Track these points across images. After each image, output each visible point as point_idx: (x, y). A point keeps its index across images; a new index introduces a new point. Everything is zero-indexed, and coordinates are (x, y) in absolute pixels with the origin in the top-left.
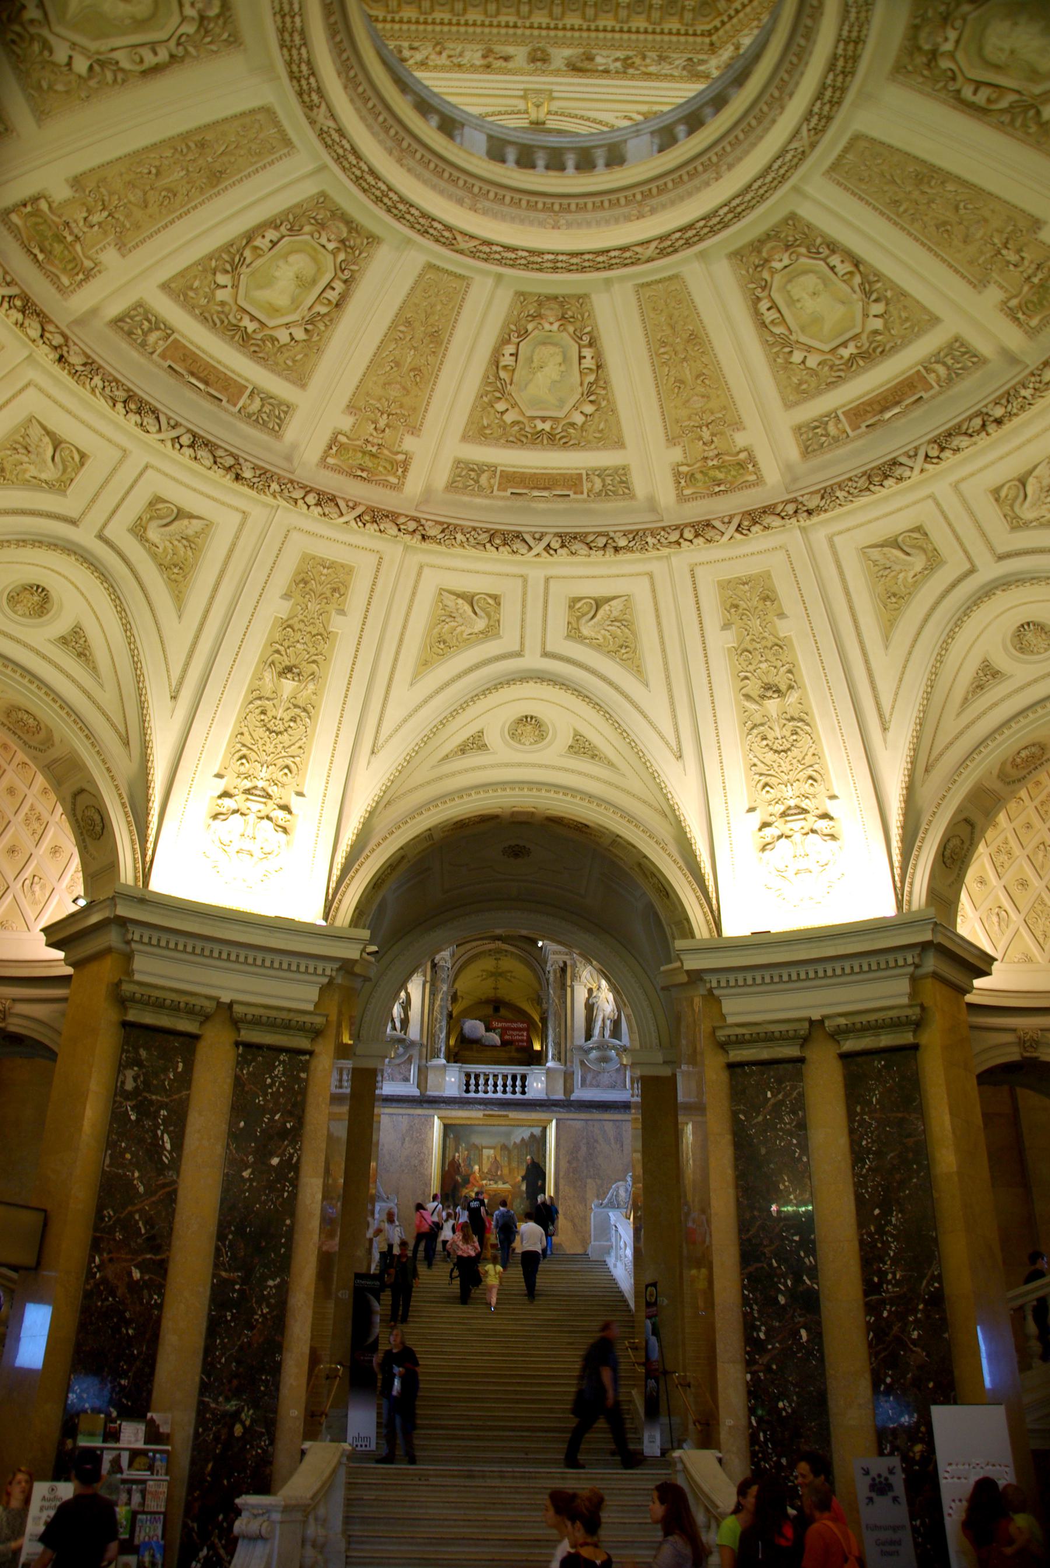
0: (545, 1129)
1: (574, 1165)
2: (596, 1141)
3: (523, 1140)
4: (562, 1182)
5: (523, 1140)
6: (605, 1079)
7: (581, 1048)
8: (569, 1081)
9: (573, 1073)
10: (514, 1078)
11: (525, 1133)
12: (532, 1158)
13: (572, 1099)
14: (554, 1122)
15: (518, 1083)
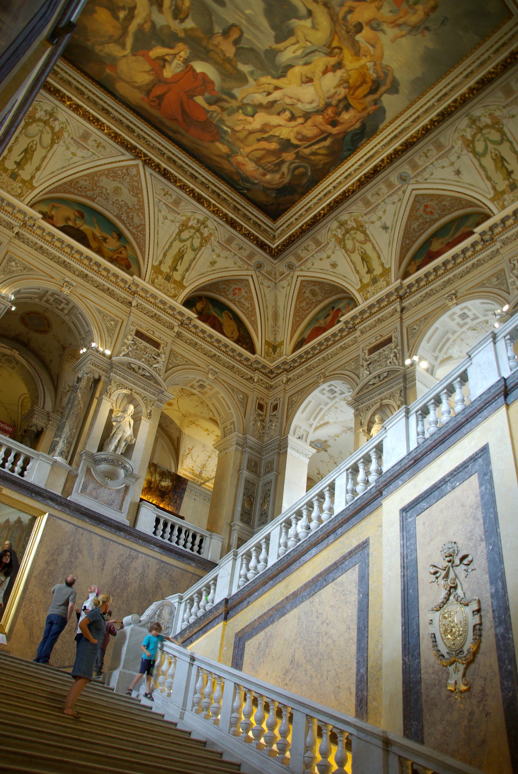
0: (34, 519)
1: (52, 568)
2: (80, 551)
3: (8, 521)
4: (33, 581)
5: (8, 521)
6: (104, 494)
7: (91, 456)
8: (70, 482)
9: (76, 476)
10: (17, 457)
11: (13, 515)
12: (11, 544)
13: (68, 498)
14: (46, 516)
15: (20, 463)
